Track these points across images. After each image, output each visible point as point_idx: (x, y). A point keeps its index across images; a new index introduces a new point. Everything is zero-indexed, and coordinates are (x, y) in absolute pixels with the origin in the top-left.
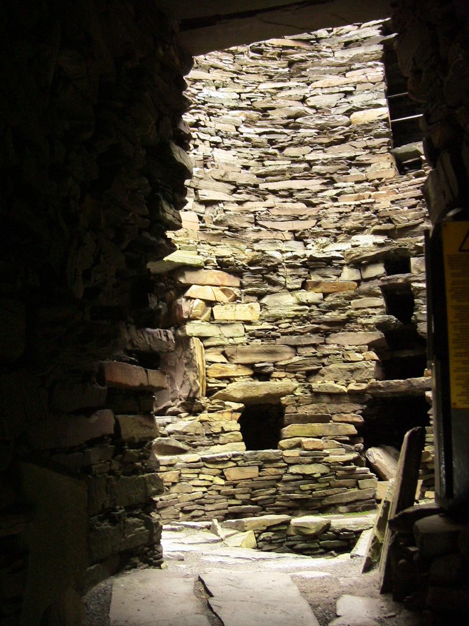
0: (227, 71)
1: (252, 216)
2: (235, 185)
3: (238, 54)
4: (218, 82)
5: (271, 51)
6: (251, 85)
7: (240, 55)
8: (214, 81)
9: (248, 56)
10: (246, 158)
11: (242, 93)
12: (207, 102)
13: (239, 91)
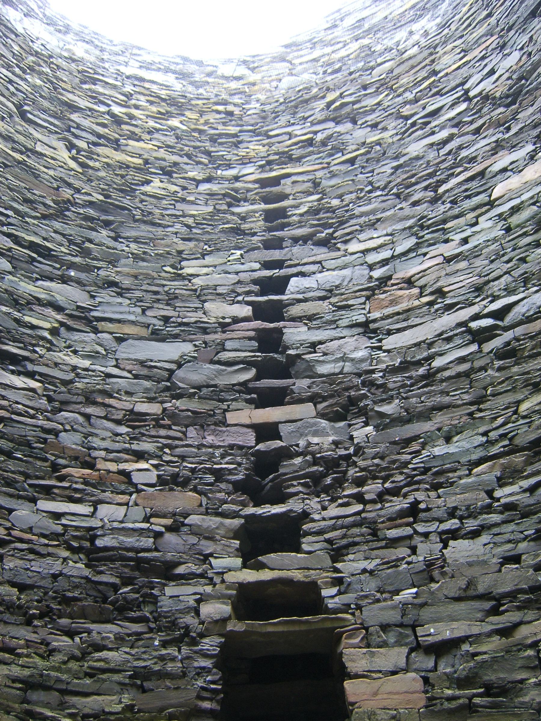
0: (458, 406)
1: (530, 652)
2: (493, 598)
3: (476, 373)
4: (446, 429)
5: (529, 344)
6: (503, 412)
7: (478, 374)
8: (439, 429)
9: (493, 369)
10: (509, 541)
11: (490, 431)
12: (429, 469)
13: (482, 430)
